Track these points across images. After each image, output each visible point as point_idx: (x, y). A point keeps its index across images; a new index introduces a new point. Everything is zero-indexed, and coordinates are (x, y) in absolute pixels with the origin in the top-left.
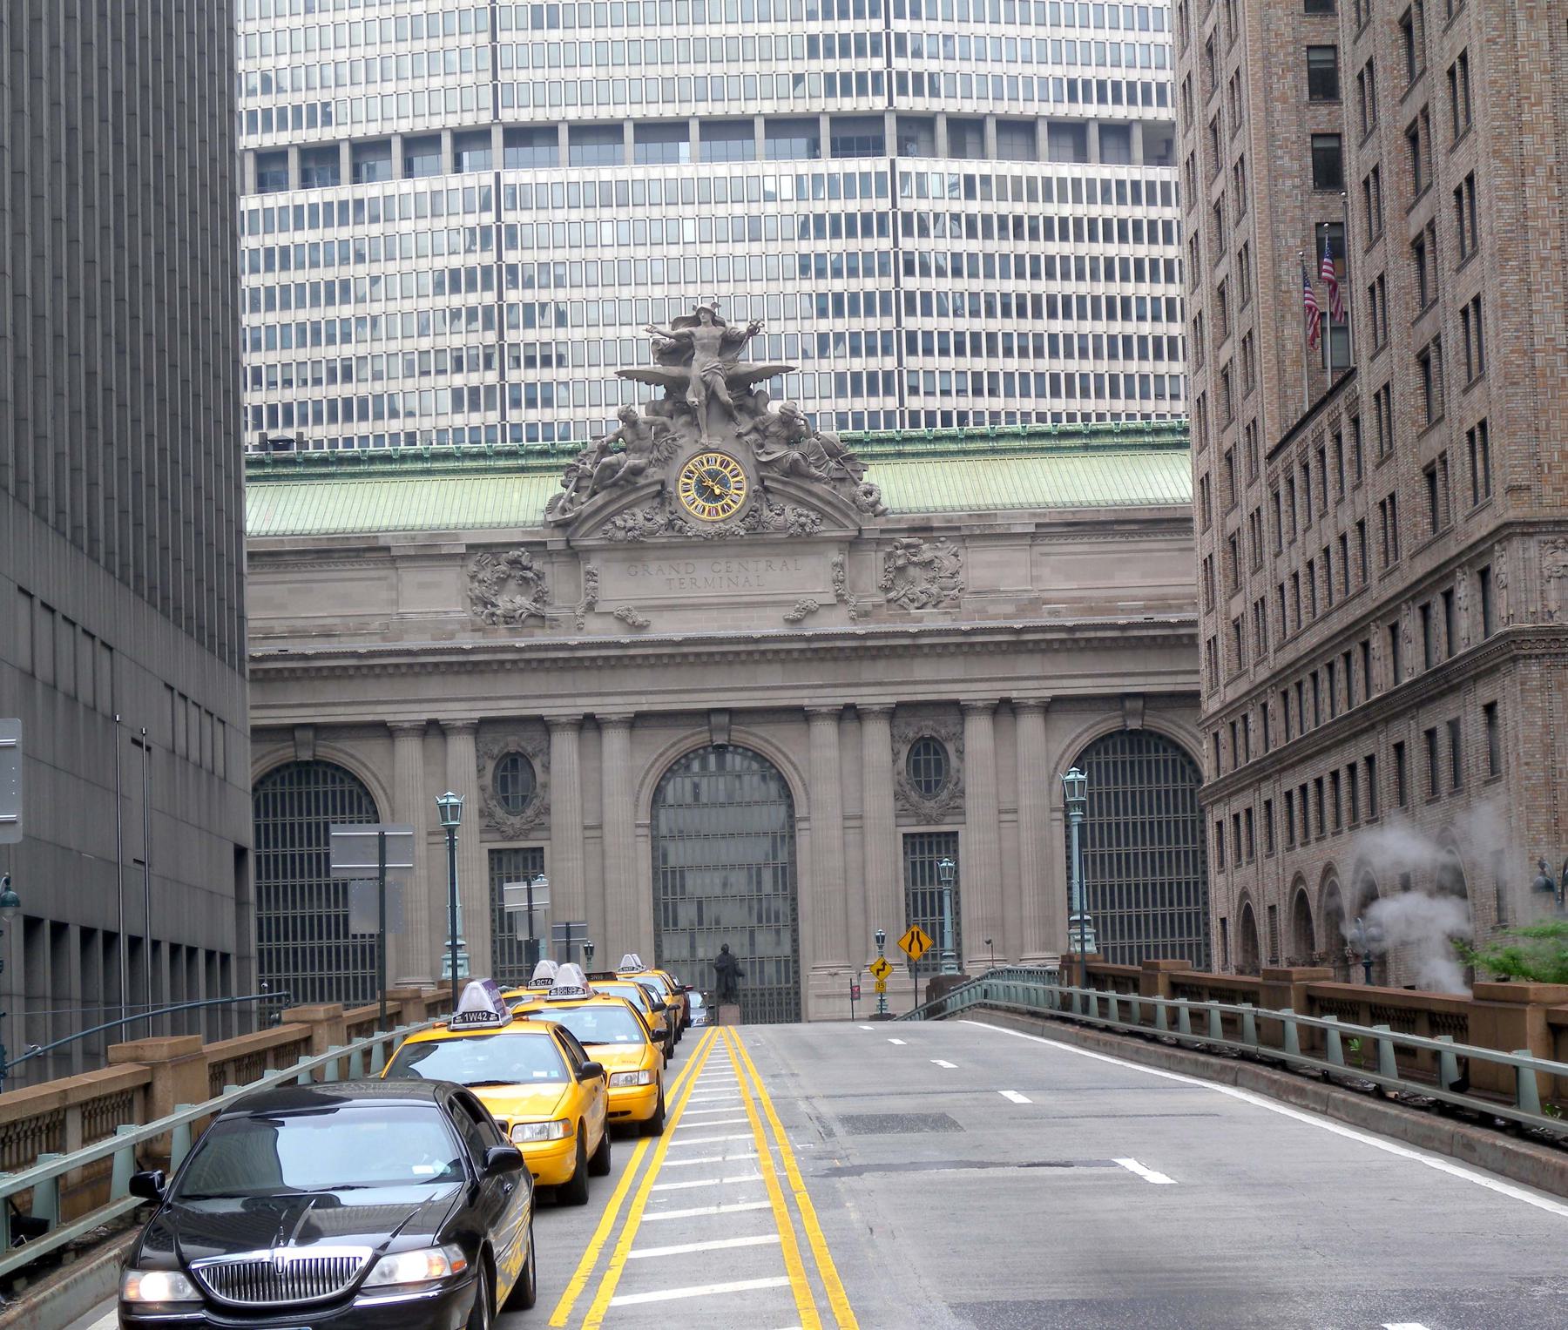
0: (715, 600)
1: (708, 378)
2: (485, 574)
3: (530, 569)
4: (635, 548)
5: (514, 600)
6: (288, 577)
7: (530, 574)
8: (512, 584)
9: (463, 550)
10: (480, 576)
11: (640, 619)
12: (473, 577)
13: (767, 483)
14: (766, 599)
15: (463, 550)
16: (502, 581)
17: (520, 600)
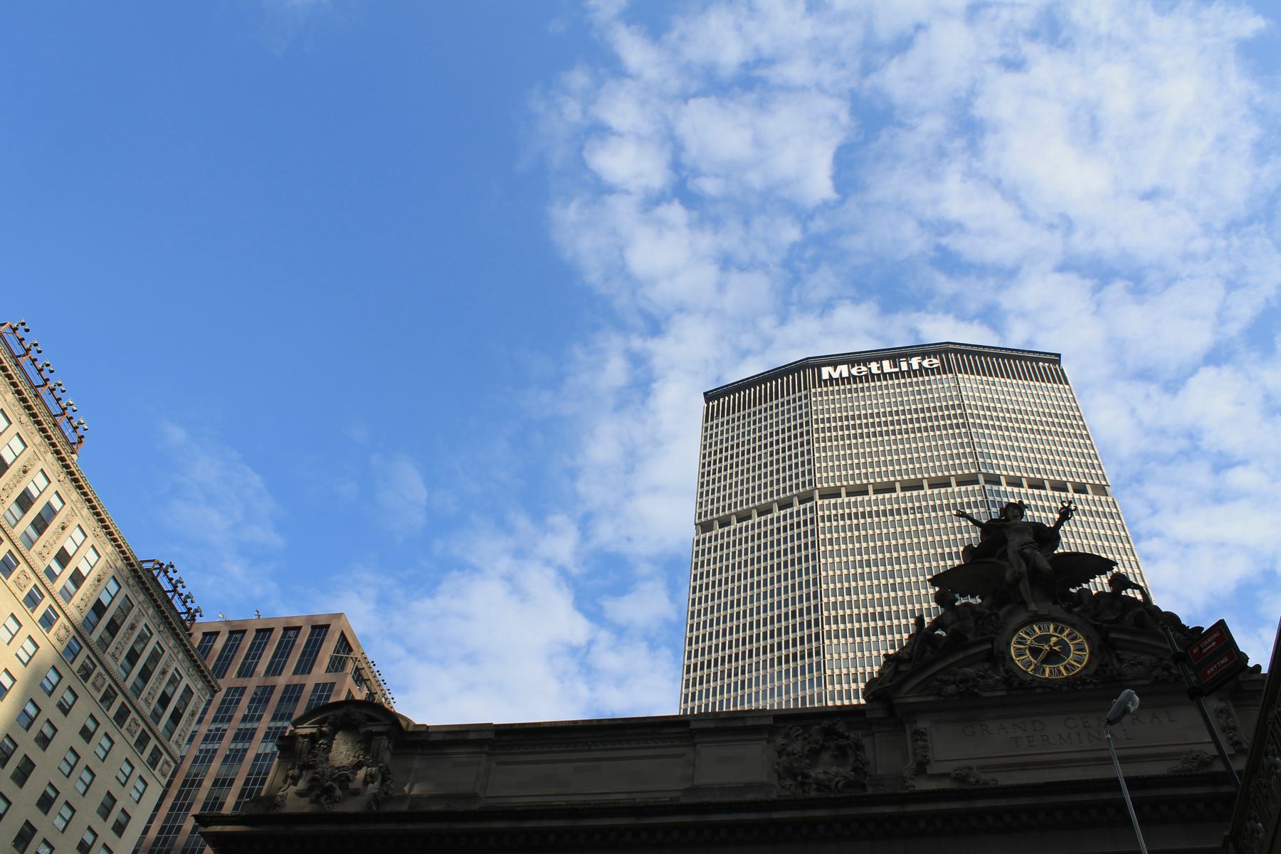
0: (1077, 756)
1: (1028, 551)
2: (797, 747)
3: (848, 738)
4: (968, 705)
5: (826, 769)
6: (576, 756)
7: (844, 742)
8: (826, 757)
9: (771, 721)
10: (789, 749)
11: (984, 777)
12: (780, 753)
13: (1113, 635)
14: (1140, 752)
15: (771, 721)
16: (814, 754)
17: (834, 769)
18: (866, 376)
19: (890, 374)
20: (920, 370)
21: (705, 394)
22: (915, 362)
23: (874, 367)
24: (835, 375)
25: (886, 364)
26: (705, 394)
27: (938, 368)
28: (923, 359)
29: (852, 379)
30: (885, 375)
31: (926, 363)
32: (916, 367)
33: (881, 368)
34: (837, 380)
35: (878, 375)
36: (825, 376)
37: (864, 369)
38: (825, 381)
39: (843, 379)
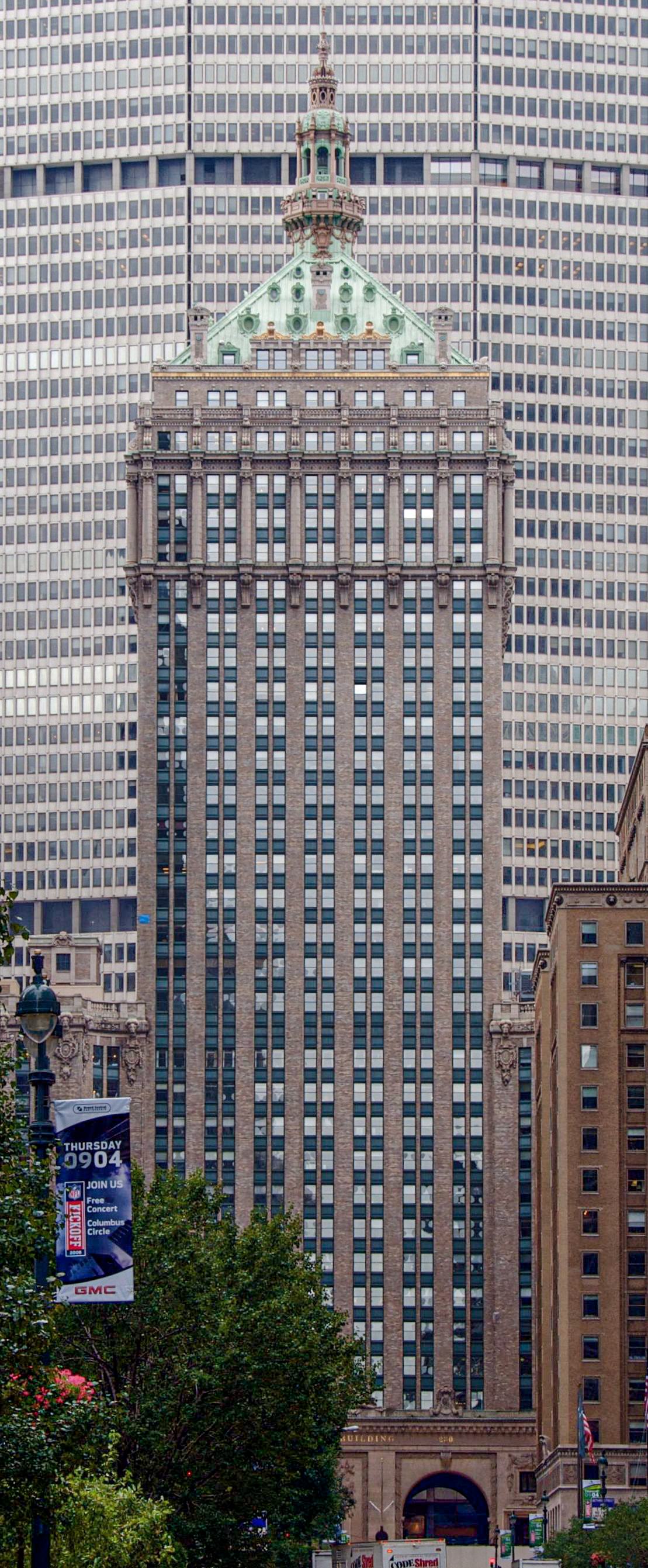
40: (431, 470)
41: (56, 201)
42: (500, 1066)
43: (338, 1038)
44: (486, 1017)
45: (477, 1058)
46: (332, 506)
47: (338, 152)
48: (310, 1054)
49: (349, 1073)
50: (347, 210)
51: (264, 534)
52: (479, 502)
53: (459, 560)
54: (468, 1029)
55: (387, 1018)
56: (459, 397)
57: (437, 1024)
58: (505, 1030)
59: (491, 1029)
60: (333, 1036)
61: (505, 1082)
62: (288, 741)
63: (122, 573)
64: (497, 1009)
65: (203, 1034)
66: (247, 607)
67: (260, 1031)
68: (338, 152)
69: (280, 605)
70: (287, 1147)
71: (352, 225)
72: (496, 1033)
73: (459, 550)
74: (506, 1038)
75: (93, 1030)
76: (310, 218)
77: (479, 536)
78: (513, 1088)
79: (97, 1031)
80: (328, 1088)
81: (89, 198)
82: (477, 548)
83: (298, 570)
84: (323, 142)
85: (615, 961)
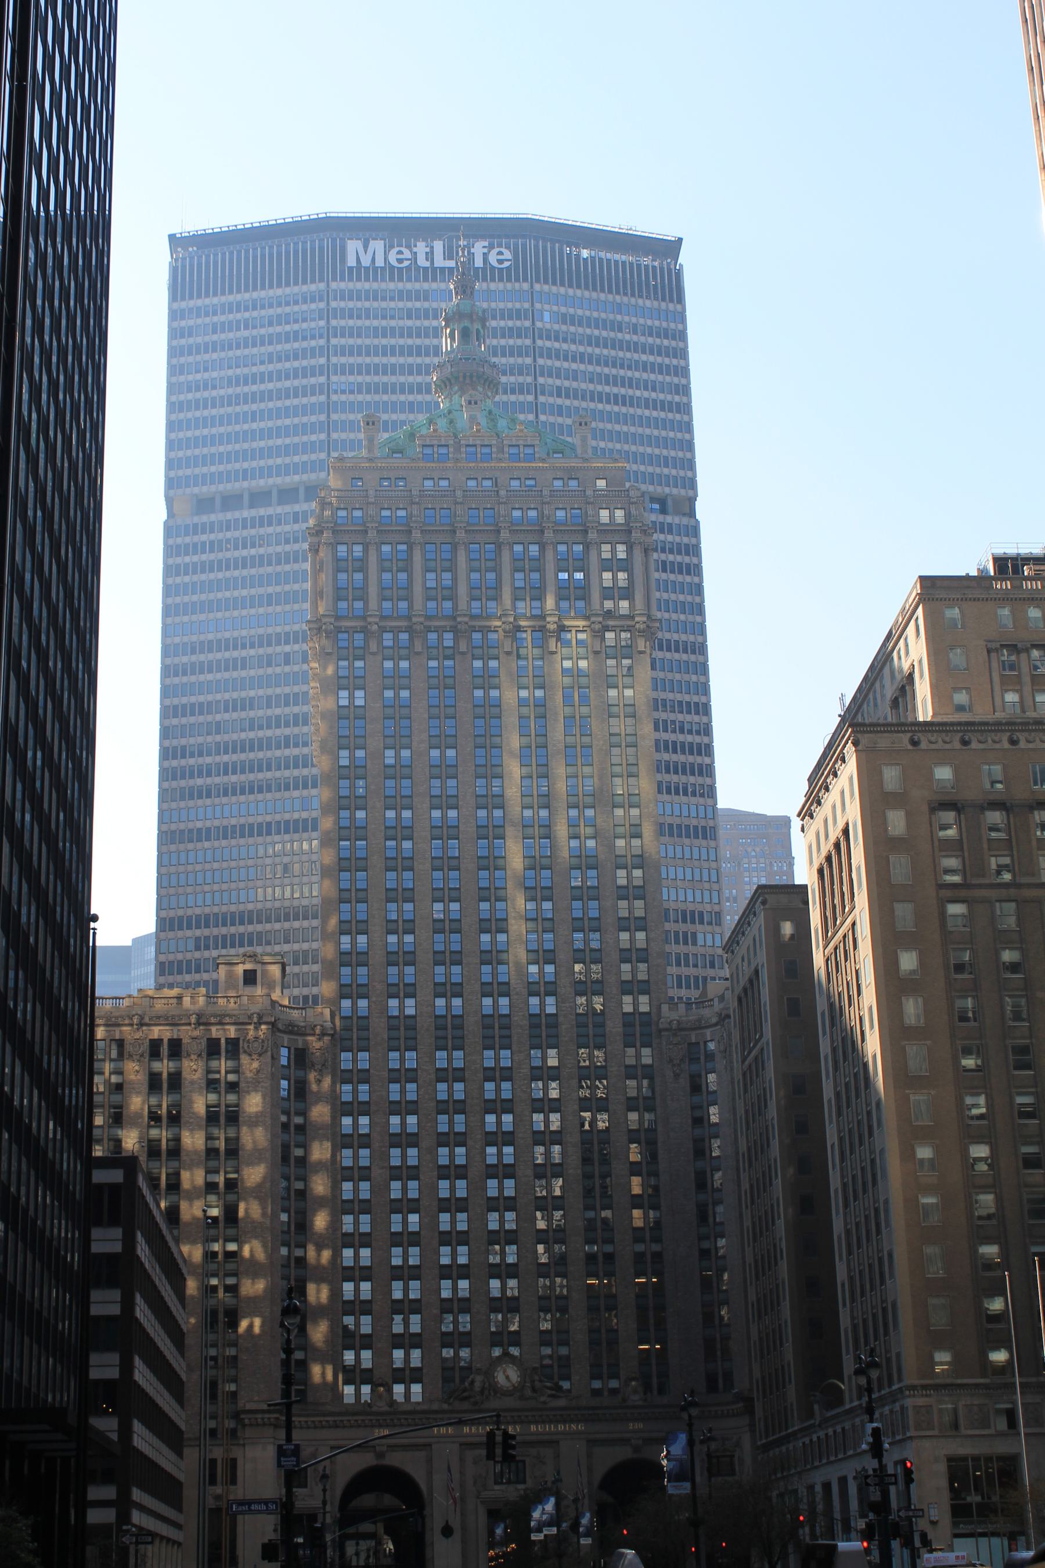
18: (408, 268)
19: (442, 269)
20: (484, 269)
21: (172, 238)
22: (479, 248)
23: (421, 248)
24: (366, 261)
25: (438, 246)
26: (172, 238)
27: (508, 268)
28: (491, 247)
29: (392, 272)
30: (434, 269)
31: (493, 259)
32: (479, 262)
33: (430, 256)
34: (367, 269)
35: (425, 269)
36: (351, 262)
37: (407, 254)
38: (351, 269)
39: (376, 269)
40: (580, 539)
41: (229, 515)
42: (671, 1061)
43: (515, 1038)
44: (654, 1018)
45: (647, 1056)
46: (493, 570)
47: (478, 331)
48: (489, 1053)
49: (526, 1071)
50: (487, 370)
51: (433, 593)
52: (626, 565)
53: (609, 612)
54: (638, 1028)
55: (561, 1019)
56: (601, 484)
57: (609, 1024)
58: (674, 1026)
59: (661, 1026)
60: (510, 1037)
61: (677, 1076)
62: (460, 769)
63: (305, 627)
64: (665, 1008)
65: (386, 1037)
66: (418, 653)
67: (440, 1033)
68: (478, 331)
69: (449, 652)
70: (469, 1142)
71: (492, 385)
72: (667, 1030)
73: (608, 604)
74: (675, 1035)
75: (279, 1031)
76: (457, 378)
77: (627, 593)
78: (684, 1082)
79: (284, 1032)
80: (506, 1085)
81: (253, 512)
82: (624, 604)
83: (466, 619)
84: (466, 323)
85: (925, 808)
